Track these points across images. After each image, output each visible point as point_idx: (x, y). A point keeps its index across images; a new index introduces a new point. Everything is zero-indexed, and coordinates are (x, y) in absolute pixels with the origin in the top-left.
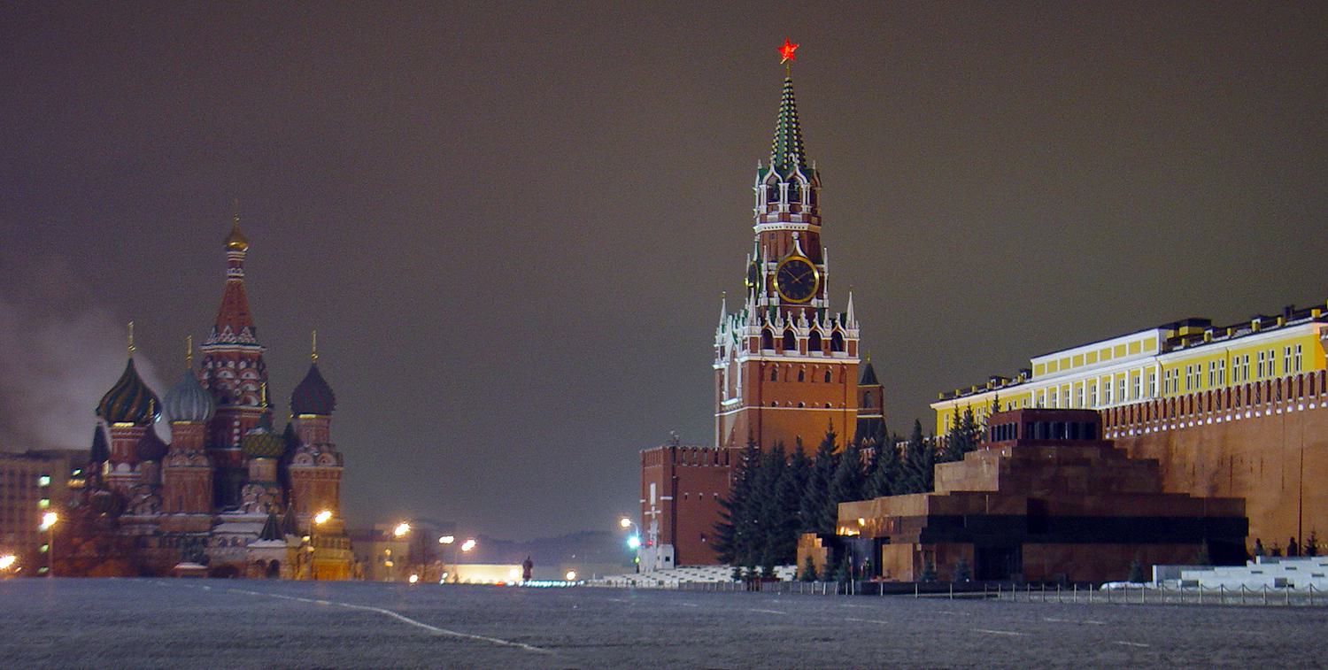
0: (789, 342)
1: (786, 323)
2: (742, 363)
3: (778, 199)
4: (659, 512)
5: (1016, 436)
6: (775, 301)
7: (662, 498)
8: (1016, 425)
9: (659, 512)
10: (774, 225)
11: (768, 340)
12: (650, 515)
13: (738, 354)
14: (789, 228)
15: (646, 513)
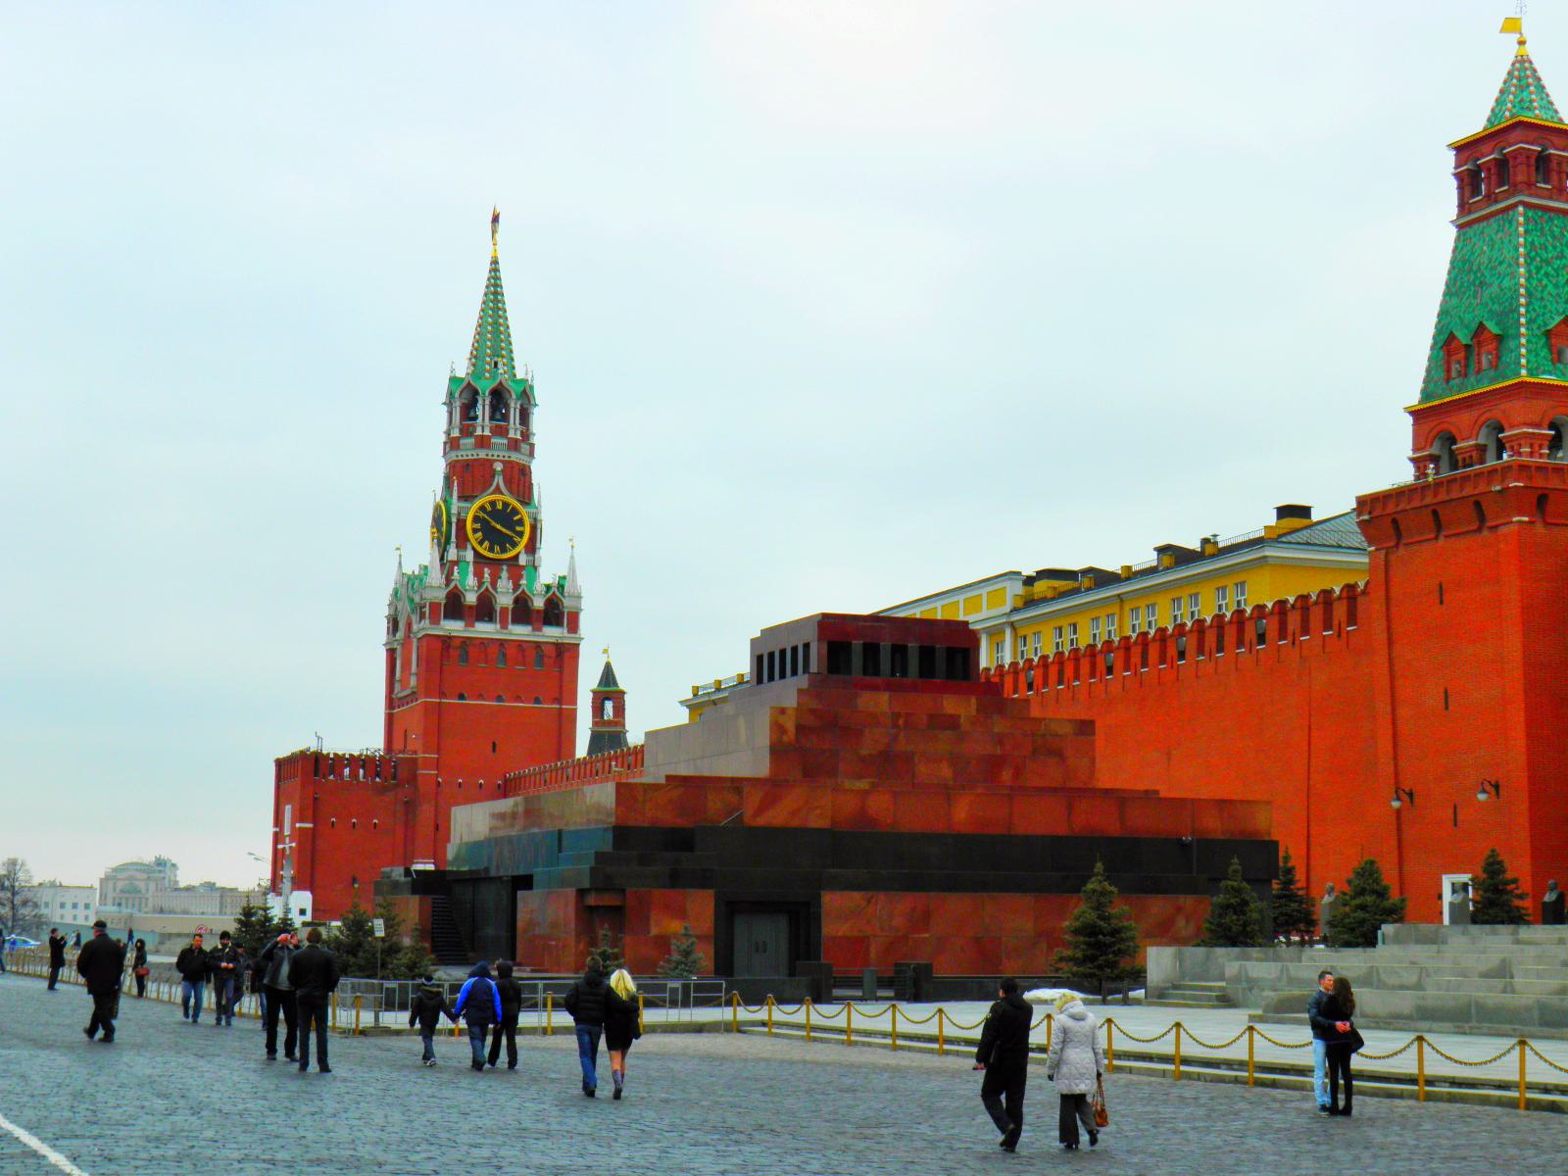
0: (485, 610)
1: (481, 584)
2: (419, 639)
3: (475, 418)
4: (294, 845)
5: (806, 669)
6: (469, 555)
7: (298, 825)
8: (807, 646)
9: (294, 845)
10: (469, 453)
11: (454, 606)
12: (284, 849)
13: (415, 627)
14: (490, 457)
15: (280, 847)
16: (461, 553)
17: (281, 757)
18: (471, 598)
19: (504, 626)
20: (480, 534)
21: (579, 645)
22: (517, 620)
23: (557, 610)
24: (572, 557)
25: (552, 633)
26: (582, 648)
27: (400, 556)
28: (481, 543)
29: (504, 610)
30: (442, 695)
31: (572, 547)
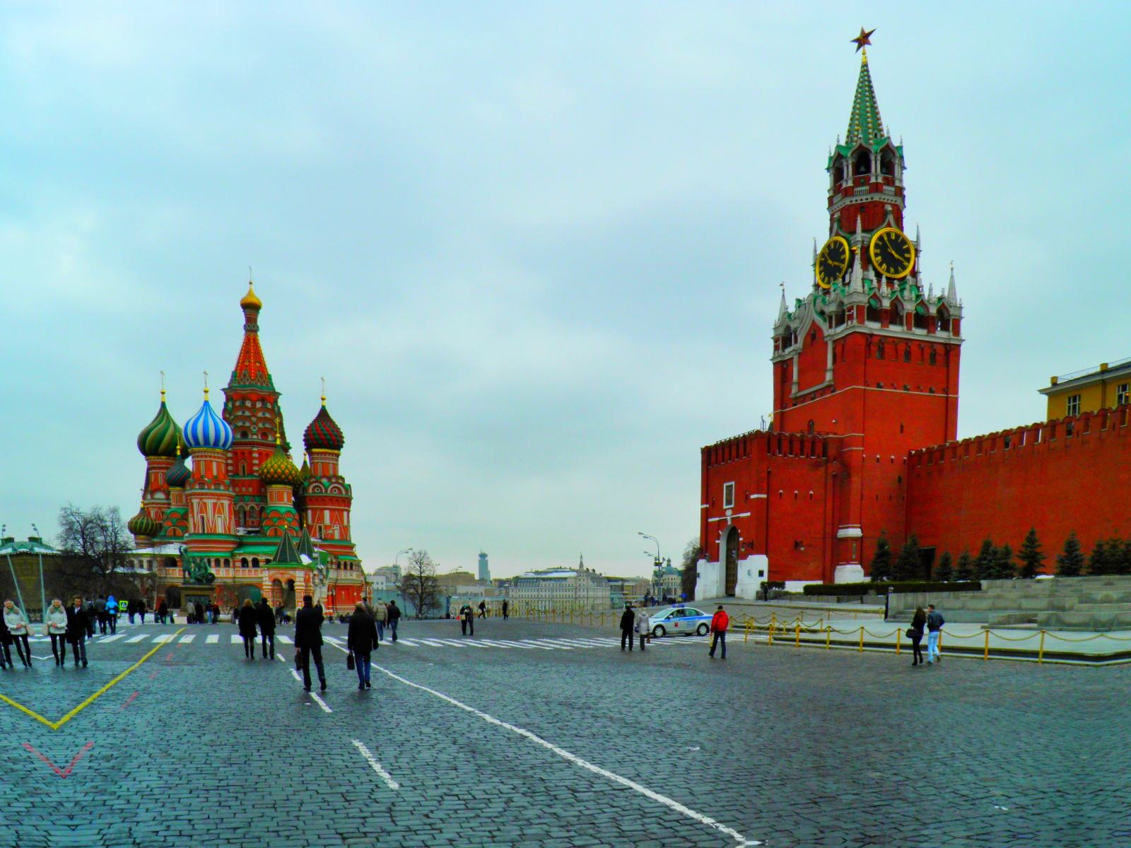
0: (893, 316)
6: (872, 274)
16: (866, 273)
17: (711, 443)
18: (886, 304)
19: (909, 328)
20: (879, 258)
21: (959, 346)
22: (918, 325)
23: (945, 316)
24: (952, 277)
25: (941, 336)
26: (962, 348)
27: (783, 290)
28: (881, 265)
29: (909, 314)
30: (866, 384)
31: (952, 269)
